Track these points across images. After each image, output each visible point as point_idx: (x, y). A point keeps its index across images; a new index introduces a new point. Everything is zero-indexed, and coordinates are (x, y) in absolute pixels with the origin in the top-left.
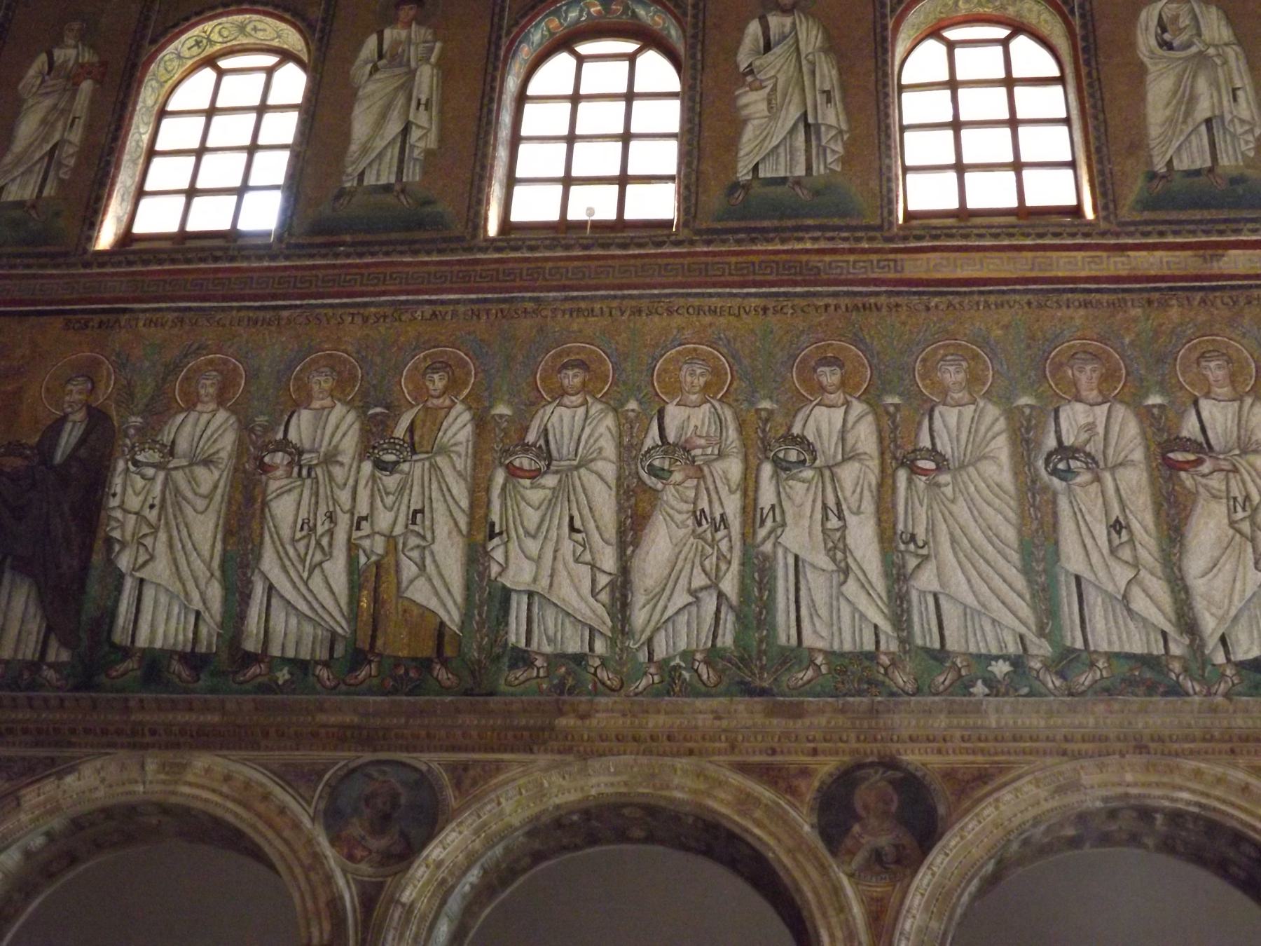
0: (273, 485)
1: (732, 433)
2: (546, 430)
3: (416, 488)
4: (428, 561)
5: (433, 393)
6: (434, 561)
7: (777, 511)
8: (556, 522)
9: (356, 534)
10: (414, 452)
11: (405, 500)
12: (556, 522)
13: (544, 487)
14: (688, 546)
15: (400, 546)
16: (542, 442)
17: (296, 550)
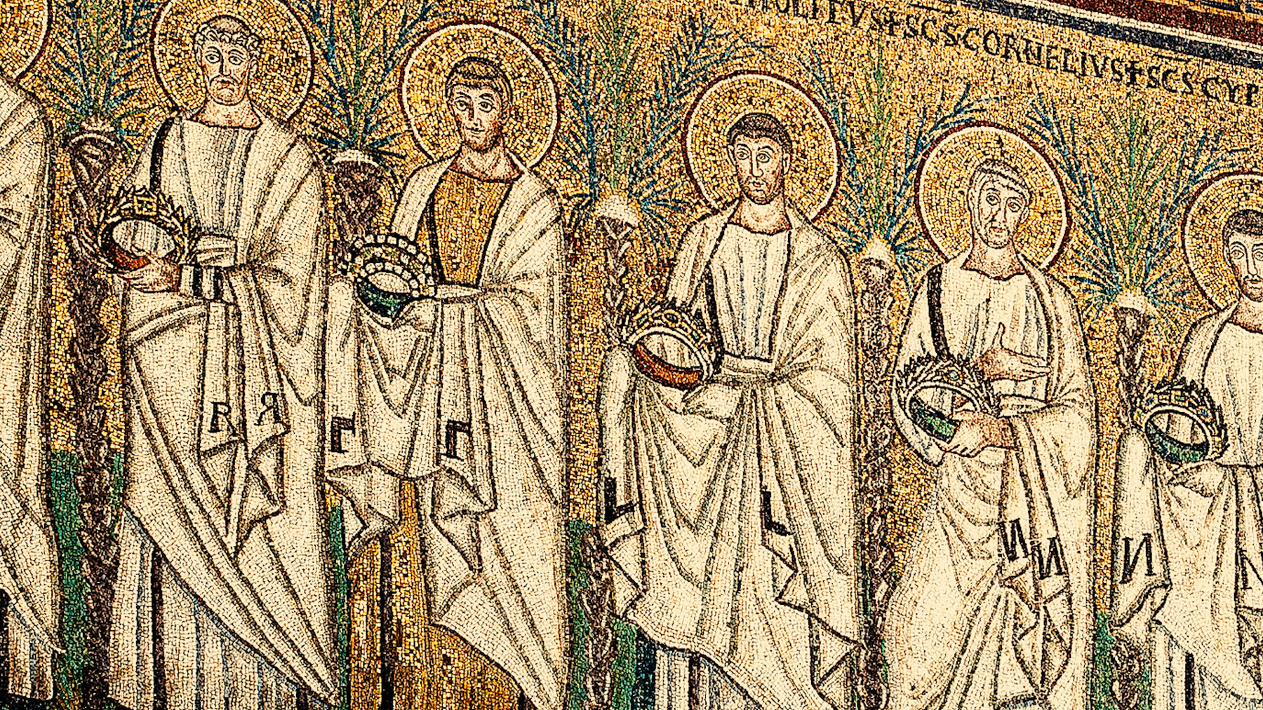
0: (143, 306)
1: (1072, 361)
2: (709, 277)
3: (451, 370)
4: (487, 551)
5: (468, 135)
6: (500, 552)
7: (1156, 551)
8: (735, 496)
9: (333, 460)
10: (441, 280)
11: (430, 397)
12: (735, 496)
13: (708, 415)
14: (991, 598)
15: (427, 506)
16: (701, 304)
17: (207, 478)
